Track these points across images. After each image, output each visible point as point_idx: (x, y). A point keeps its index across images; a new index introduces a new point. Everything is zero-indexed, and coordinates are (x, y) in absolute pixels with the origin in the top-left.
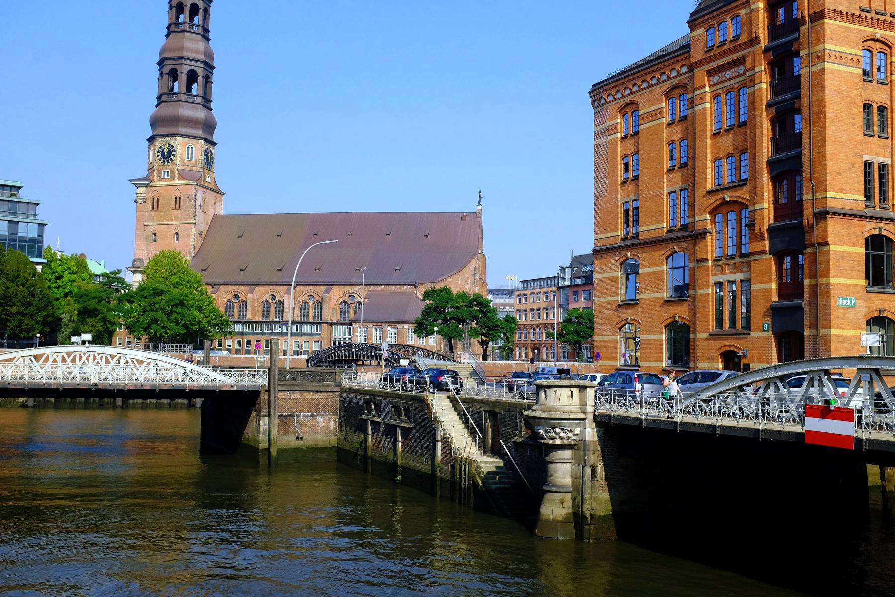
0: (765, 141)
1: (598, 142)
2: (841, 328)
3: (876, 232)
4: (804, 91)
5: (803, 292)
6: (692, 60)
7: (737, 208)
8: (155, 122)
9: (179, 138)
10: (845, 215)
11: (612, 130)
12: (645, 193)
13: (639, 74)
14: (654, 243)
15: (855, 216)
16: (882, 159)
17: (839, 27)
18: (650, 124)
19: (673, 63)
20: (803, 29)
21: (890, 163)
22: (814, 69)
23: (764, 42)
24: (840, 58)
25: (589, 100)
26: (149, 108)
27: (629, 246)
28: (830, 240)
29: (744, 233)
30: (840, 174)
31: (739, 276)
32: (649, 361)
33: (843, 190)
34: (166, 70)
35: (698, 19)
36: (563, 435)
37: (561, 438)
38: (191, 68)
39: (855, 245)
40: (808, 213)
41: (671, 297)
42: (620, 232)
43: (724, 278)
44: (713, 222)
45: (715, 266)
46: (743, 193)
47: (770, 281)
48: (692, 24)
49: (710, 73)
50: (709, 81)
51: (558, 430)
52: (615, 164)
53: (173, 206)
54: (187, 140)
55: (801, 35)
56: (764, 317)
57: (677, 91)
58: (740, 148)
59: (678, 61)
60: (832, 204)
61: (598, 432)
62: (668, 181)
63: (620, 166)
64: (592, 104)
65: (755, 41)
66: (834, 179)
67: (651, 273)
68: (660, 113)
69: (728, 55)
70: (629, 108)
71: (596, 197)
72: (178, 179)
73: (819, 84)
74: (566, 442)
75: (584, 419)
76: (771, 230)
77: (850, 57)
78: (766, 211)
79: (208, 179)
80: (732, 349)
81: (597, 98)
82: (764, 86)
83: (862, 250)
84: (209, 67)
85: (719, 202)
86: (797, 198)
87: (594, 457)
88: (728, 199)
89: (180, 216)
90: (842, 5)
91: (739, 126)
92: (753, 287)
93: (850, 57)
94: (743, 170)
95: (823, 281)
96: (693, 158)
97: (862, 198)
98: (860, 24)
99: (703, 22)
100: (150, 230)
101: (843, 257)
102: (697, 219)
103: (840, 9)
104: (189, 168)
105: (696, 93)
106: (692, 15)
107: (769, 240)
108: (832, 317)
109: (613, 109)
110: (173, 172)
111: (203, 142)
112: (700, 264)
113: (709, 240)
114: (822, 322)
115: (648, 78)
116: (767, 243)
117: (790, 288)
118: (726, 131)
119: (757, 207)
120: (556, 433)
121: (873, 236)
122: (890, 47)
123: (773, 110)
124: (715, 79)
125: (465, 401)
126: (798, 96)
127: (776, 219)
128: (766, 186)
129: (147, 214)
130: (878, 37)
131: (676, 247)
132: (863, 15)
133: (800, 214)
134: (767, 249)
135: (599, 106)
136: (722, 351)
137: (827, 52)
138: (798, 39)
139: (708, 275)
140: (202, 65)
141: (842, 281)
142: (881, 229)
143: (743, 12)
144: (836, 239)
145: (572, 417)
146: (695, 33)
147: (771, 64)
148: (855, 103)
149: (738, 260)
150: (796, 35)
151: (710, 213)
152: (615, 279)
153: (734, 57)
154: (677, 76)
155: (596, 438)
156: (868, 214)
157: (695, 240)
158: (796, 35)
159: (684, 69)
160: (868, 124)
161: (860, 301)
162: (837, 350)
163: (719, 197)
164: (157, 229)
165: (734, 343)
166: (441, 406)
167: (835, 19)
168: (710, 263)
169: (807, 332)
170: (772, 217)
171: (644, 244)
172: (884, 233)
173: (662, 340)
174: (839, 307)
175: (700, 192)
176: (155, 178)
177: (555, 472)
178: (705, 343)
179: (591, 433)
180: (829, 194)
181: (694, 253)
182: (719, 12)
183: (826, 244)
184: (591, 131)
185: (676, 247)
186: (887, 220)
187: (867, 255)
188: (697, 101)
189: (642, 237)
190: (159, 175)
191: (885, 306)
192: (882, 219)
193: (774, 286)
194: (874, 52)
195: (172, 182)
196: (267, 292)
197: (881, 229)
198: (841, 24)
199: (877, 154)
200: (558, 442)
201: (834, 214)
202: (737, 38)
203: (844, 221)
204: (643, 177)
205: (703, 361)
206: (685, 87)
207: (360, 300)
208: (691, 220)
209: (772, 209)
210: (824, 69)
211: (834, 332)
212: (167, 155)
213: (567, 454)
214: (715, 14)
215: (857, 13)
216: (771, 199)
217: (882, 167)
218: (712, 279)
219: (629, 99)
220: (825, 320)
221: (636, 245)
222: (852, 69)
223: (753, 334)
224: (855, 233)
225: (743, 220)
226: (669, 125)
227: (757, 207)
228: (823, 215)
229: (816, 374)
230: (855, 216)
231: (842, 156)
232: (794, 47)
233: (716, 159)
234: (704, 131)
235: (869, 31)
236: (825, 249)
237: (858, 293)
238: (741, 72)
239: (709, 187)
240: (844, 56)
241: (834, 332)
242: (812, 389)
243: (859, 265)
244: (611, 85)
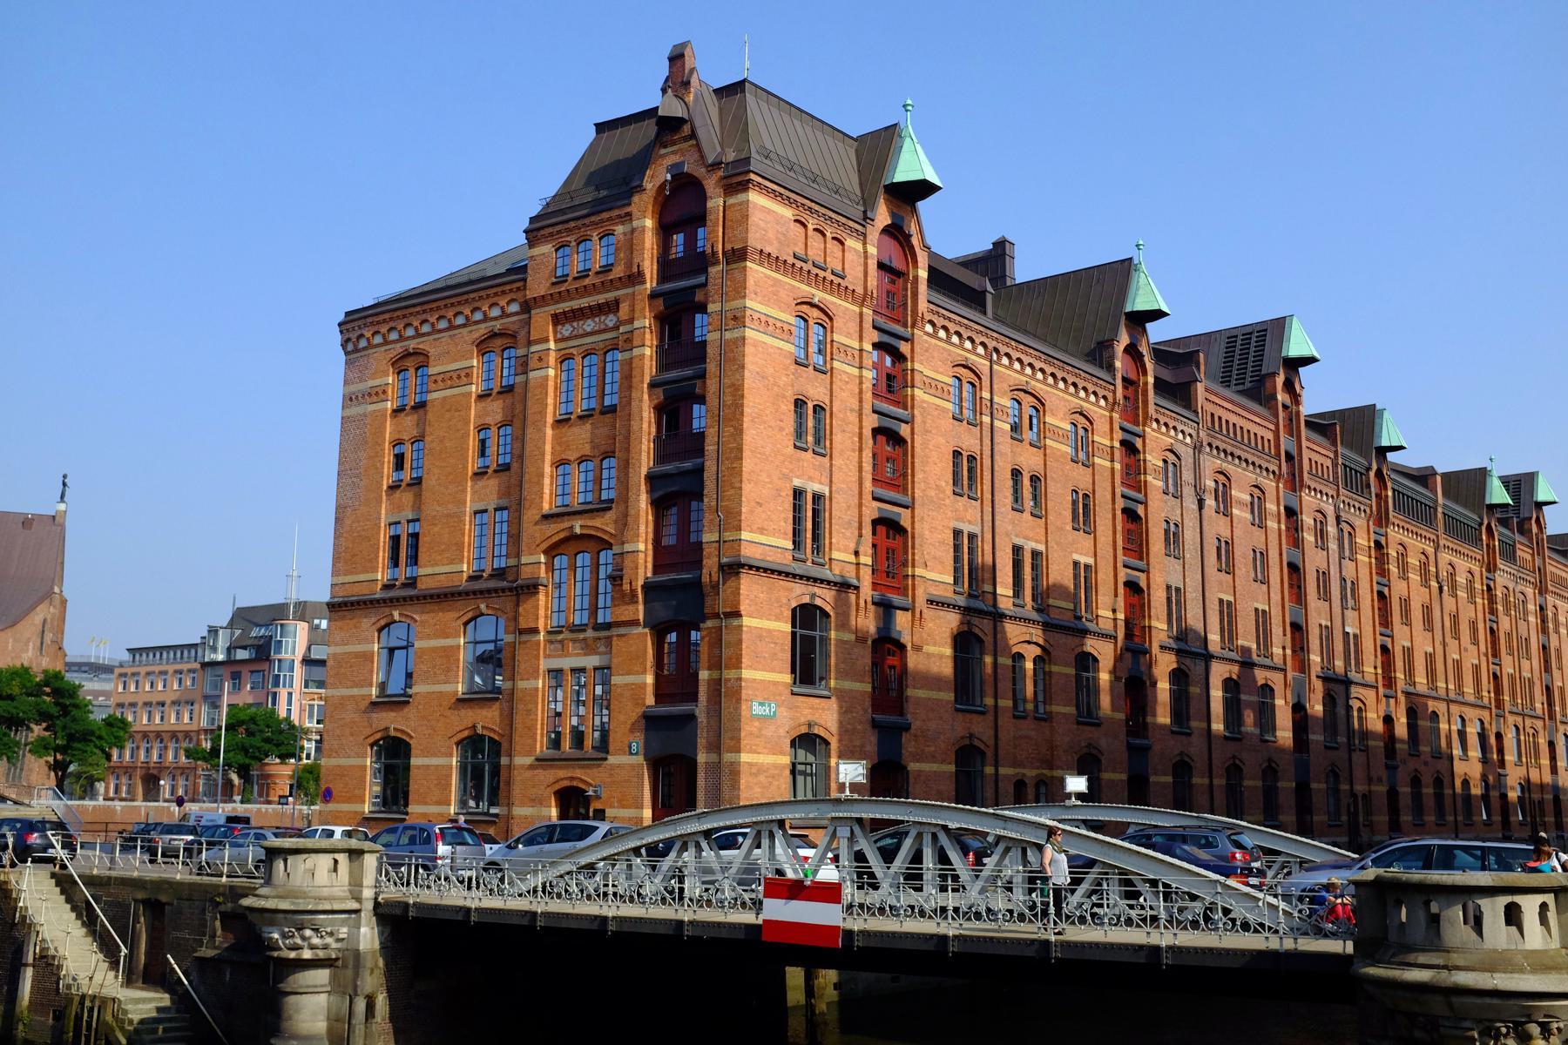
0: (645, 440)
1: (348, 412)
3: (806, 600)
4: (711, 367)
5: (696, 693)
6: (529, 295)
7: (591, 545)
10: (765, 570)
11: (378, 394)
12: (431, 509)
13: (434, 305)
14: (444, 597)
15: (780, 573)
16: (817, 487)
17: (769, 277)
18: (448, 392)
19: (496, 294)
20: (713, 270)
22: (728, 335)
23: (650, 284)
24: (766, 324)
25: (338, 338)
27: (398, 600)
28: (742, 608)
29: (601, 590)
30: (760, 504)
31: (592, 661)
32: (426, 803)
33: (764, 534)
35: (543, 228)
36: (316, 941)
37: (312, 947)
39: (778, 619)
40: (710, 564)
42: (382, 575)
43: (566, 663)
44: (550, 567)
45: (551, 642)
46: (605, 524)
47: (644, 672)
48: (534, 233)
49: (557, 319)
50: (555, 332)
51: (308, 933)
52: (378, 455)
55: (711, 280)
56: (632, 731)
57: (498, 342)
58: (603, 449)
59: (503, 292)
60: (748, 553)
61: (381, 933)
62: (474, 493)
63: (388, 459)
64: (344, 346)
65: (636, 278)
66: (752, 512)
67: (434, 650)
68: (467, 375)
69: (590, 295)
70: (410, 361)
71: (341, 510)
73: (735, 359)
74: (321, 954)
75: (357, 911)
76: (647, 587)
77: (779, 324)
78: (642, 556)
80: (575, 783)
81: (354, 336)
82: (648, 352)
83: (788, 628)
85: (562, 535)
86: (693, 538)
87: (373, 981)
88: (578, 531)
90: (771, 244)
91: (602, 413)
92: (615, 680)
93: (779, 324)
94: (605, 484)
95: (729, 674)
96: (521, 457)
98: (794, 278)
99: (551, 234)
101: (760, 637)
102: (524, 560)
103: (767, 249)
105: (533, 349)
106: (532, 220)
107: (645, 603)
109: (381, 358)
112: (524, 638)
113: (542, 597)
114: (726, 741)
115: (450, 314)
116: (641, 607)
117: (677, 682)
118: (580, 417)
119: (628, 547)
120: (304, 938)
121: (802, 606)
122: (831, 319)
123: (660, 391)
124: (566, 330)
125: (91, 881)
126: (702, 376)
127: (657, 568)
128: (643, 514)
130: (816, 300)
131: (483, 606)
132: (799, 264)
133: (698, 564)
134: (641, 617)
135: (356, 350)
136: (557, 787)
137: (748, 313)
138: (705, 285)
143: (620, 229)
145: (337, 907)
146: (537, 251)
147: (661, 319)
148: (784, 396)
149: (590, 633)
150: (702, 279)
151: (545, 552)
152: (367, 657)
153: (601, 298)
154: (501, 317)
155: (377, 945)
156: (798, 572)
157: (518, 595)
158: (702, 279)
159: (514, 308)
160: (800, 433)
163: (566, 525)
165: (578, 773)
166: (35, 892)
167: (761, 264)
168: (542, 636)
169: (702, 758)
170: (650, 566)
171: (425, 597)
172: (818, 602)
175: (530, 515)
177: (297, 1011)
178: (528, 774)
179: (368, 936)
180: (745, 535)
181: (515, 619)
182: (580, 223)
183: (738, 615)
184: (338, 391)
185: (483, 606)
186: (822, 581)
187: (794, 634)
188: (533, 363)
191: (815, 718)
192: (816, 580)
193: (650, 679)
194: (811, 322)
197: (813, 596)
198: (769, 272)
199: (811, 479)
200: (307, 954)
201: (751, 567)
202: (607, 269)
205: (522, 805)
206: (514, 336)
208: (512, 562)
209: (650, 553)
210: (744, 338)
211: (745, 757)
213: (322, 976)
214: (572, 224)
215: (791, 260)
216: (651, 536)
218: (544, 664)
219: (412, 345)
221: (411, 598)
222: (781, 344)
223: (612, 760)
224: (778, 600)
225: (602, 568)
226: (480, 397)
227: (628, 547)
228: (733, 569)
229: (765, 826)
230: (780, 573)
231: (764, 477)
232: (699, 297)
233: (559, 463)
234: (543, 413)
235: (806, 290)
236: (735, 622)
238: (611, 324)
239: (546, 507)
240: (771, 321)
241: (745, 757)
242: (757, 851)
243: (783, 650)
244: (381, 318)
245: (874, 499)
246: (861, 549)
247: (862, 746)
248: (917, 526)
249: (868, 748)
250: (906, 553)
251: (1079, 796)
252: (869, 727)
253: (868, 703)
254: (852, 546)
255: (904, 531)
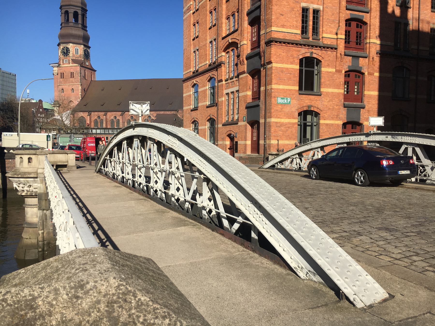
2: (279, 118)
3: (308, 55)
8: (61, 36)
9: (71, 44)
15: (293, 44)
16: (316, 6)
21: (321, 9)
26: (57, 31)
28: (272, 60)
34: (63, 11)
38: (75, 10)
39: (292, 63)
41: (211, 104)
43: (229, 91)
53: (70, 76)
54: (75, 45)
60: (275, 36)
72: (72, 63)
79: (87, 64)
83: (298, 67)
84: (84, 11)
88: (230, 41)
89: (74, 81)
95: (269, 87)
97: (299, 32)
100: (61, 87)
101: (282, 71)
104: (77, 59)
108: (272, 111)
110: (69, 60)
111: (83, 46)
113: (223, 68)
114: (268, 115)
116: (246, 66)
119: (242, 44)
121: (307, 58)
129: (59, 80)
134: (246, 70)
139: (223, 90)
140: (80, 9)
141: (281, 87)
142: (312, 53)
144: (278, 59)
161: (294, 100)
162: (275, 131)
164: (64, 87)
169: (262, 121)
172: (315, 56)
173: (206, 129)
174: (278, 104)
176: (61, 63)
177: (27, 214)
186: (316, 47)
187: (301, 71)
189: (199, 71)
190: (63, 62)
191: (313, 103)
192: (312, 46)
195: (69, 65)
196: (112, 115)
197: (312, 53)
199: (312, 3)
201: (276, 42)
203: (284, 47)
204: (200, 35)
207: (153, 118)
212: (66, 52)
213: (35, 201)
217: (316, 12)
220: (269, 113)
224: (292, 55)
227: (242, 44)
236: (269, 66)
237: (293, 95)
239: (224, 35)
243: (294, 76)
245: (347, 9)
246: (339, 32)
247: (337, 116)
248: (372, 21)
249: (341, 116)
250: (367, 33)
251: (379, 128)
252: (342, 108)
253: (342, 98)
254: (335, 31)
255: (365, 23)
